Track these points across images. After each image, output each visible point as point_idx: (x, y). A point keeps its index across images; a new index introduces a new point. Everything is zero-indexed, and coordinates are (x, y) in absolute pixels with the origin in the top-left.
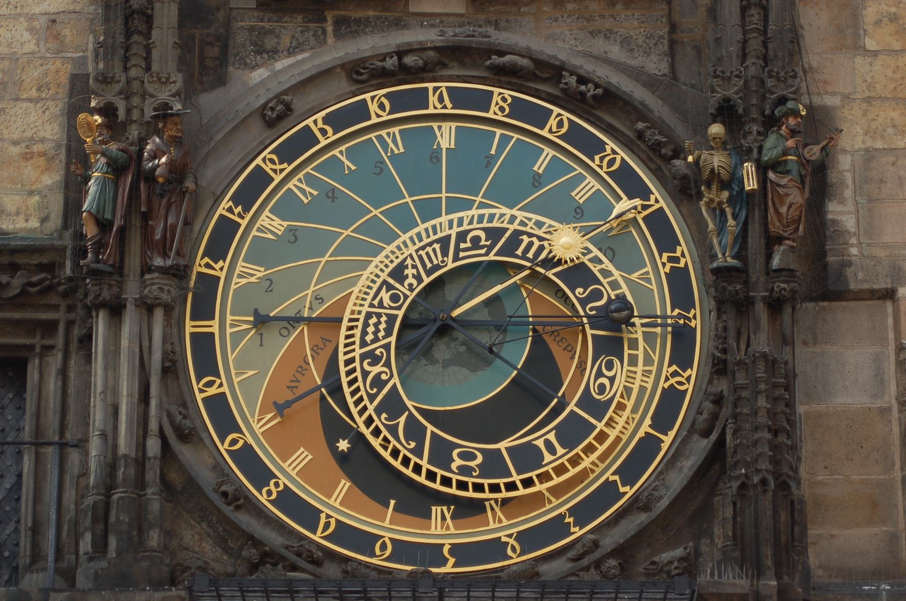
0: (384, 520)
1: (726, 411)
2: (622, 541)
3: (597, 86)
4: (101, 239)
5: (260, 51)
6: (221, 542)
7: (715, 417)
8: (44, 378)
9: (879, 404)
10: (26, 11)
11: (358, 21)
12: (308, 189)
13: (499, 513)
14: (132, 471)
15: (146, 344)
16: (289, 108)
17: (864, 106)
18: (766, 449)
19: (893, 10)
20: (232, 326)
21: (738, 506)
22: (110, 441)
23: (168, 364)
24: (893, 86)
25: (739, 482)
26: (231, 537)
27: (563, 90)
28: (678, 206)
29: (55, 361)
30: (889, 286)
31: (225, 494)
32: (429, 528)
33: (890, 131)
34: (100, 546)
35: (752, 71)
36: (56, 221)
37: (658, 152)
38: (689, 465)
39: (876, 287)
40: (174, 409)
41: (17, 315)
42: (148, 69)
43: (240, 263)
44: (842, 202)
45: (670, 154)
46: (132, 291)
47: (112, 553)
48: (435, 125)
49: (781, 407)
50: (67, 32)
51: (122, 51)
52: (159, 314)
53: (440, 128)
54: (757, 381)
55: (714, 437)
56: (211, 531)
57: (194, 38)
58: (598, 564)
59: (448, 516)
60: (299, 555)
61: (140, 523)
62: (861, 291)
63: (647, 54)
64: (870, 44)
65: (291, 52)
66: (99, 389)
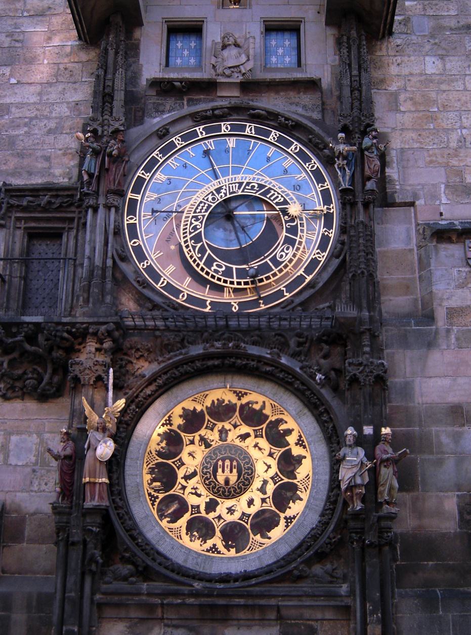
0: (204, 293)
1: (346, 247)
2: (303, 300)
3: (293, 121)
4: (90, 181)
5: (157, 111)
6: (137, 301)
7: (342, 250)
9: (409, 247)
10: (67, 100)
11: (197, 100)
12: (175, 164)
14: (100, 272)
15: (107, 222)
16: (168, 132)
17: (400, 132)
18: (363, 260)
19: (411, 96)
20: (144, 217)
21: (352, 283)
23: (116, 230)
24: (412, 124)
25: (352, 274)
26: (141, 299)
27: (279, 123)
29: (73, 233)
30: (412, 201)
31: (138, 282)
32: (223, 297)
33: (411, 141)
34: (87, 301)
35: (356, 114)
37: (317, 146)
39: (407, 201)
40: (118, 248)
41: (58, 215)
42: (111, 115)
43: (148, 192)
44: (393, 168)
45: (322, 147)
46: (102, 200)
47: (91, 305)
48: (227, 139)
49: (369, 244)
51: (101, 109)
52: (113, 210)
53: (229, 139)
54: (359, 232)
55: (341, 258)
56: (133, 297)
58: (293, 309)
60: (169, 306)
61: (103, 293)
63: (313, 112)
64: (402, 109)
65: (169, 111)
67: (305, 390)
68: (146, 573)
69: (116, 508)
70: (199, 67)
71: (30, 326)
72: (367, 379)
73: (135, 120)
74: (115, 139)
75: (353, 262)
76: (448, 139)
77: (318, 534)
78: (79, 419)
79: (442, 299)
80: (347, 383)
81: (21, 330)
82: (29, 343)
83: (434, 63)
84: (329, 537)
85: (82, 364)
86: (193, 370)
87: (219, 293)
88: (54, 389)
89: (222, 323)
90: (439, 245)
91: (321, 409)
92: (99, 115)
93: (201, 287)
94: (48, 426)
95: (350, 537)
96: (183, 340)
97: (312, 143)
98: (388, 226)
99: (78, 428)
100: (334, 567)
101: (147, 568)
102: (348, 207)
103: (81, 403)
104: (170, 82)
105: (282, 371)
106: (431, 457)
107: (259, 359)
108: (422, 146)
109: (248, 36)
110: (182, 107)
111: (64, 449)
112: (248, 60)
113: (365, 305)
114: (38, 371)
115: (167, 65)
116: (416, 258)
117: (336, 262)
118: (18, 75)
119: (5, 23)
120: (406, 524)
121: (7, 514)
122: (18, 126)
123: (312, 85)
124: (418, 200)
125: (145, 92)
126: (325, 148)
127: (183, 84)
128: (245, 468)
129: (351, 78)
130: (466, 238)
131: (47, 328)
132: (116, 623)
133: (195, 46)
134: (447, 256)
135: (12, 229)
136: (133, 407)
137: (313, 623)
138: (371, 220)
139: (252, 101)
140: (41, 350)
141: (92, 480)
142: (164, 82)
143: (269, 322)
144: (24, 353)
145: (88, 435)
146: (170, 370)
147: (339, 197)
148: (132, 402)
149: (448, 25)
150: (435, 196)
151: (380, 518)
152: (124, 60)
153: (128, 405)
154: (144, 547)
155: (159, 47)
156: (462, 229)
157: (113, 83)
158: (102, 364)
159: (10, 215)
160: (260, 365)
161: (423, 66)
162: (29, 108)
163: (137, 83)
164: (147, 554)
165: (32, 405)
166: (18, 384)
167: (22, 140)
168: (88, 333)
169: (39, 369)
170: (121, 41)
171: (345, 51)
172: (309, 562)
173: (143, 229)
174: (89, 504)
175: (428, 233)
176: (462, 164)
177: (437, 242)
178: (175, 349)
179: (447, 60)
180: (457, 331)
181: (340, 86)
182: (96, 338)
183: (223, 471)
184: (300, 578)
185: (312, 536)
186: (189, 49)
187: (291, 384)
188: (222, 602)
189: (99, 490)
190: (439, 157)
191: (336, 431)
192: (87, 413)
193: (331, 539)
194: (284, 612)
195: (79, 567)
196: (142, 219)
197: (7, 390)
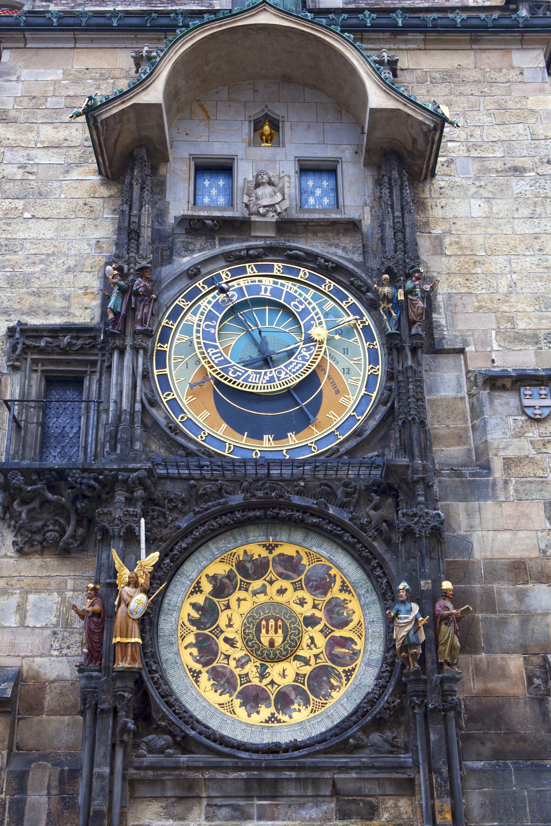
0: (242, 440)
3: (333, 263)
5: (186, 251)
6: (168, 449)
7: (389, 396)
8: (91, 386)
9: (460, 395)
11: (229, 239)
13: (294, 438)
14: (128, 417)
15: (135, 365)
17: (447, 276)
19: (457, 240)
22: (119, 406)
27: (318, 265)
28: (369, 312)
29: (96, 377)
31: (170, 428)
33: (459, 286)
34: (114, 448)
35: (400, 256)
36: (97, 320)
37: (359, 290)
38: (378, 417)
40: (147, 392)
41: (79, 358)
44: (440, 314)
46: (129, 341)
47: (118, 451)
50: (104, 246)
51: (126, 246)
52: (141, 352)
55: (389, 405)
56: (164, 444)
57: (158, 247)
58: (340, 457)
59: (271, 439)
60: (204, 454)
62: (450, 349)
64: (448, 253)
65: (200, 251)
66: (114, 383)
67: (356, 543)
68: (184, 744)
69: (151, 672)
70: (231, 204)
71: (53, 473)
72: (423, 531)
73: (162, 259)
74: (142, 277)
75: (400, 408)
76: (498, 285)
77: (376, 698)
78: (108, 573)
79: (497, 449)
80: (400, 535)
81: (41, 477)
82: (50, 492)
83: (480, 206)
84: (387, 702)
85: (111, 514)
86: (232, 522)
87: (258, 441)
88: (78, 542)
89: (263, 471)
90: (493, 393)
91: (374, 563)
92: (125, 252)
93: (238, 435)
94: (70, 584)
95: (411, 701)
96: (220, 489)
97: (354, 286)
98: (438, 374)
99: (108, 584)
100: (394, 735)
101: (186, 737)
102: (395, 353)
103: (109, 556)
104: (201, 220)
105: (329, 523)
106: (493, 616)
107: (305, 510)
108: (469, 291)
109: (282, 175)
110: (214, 247)
111: (92, 605)
112: (284, 199)
113: (417, 453)
114: (60, 523)
115: (195, 204)
116: (468, 406)
117: (383, 409)
118: (33, 209)
119: (16, 154)
120: (470, 687)
121: (24, 682)
122: (34, 263)
123: (353, 226)
124: (468, 346)
125: (173, 230)
126: (368, 291)
127: (215, 222)
128: (291, 628)
129: (394, 219)
130: (520, 386)
131: (71, 474)
132: (150, 803)
133: (224, 185)
134: (501, 404)
135: (27, 372)
136: (167, 561)
137: (372, 799)
138: (419, 364)
139: (289, 241)
140: (63, 499)
141: (125, 640)
142: (195, 220)
143: (315, 471)
144: (45, 502)
145: (118, 591)
146: (207, 522)
147: (384, 341)
148: (166, 555)
149: (494, 167)
150: (486, 343)
151: (443, 681)
152: (150, 195)
153: (161, 559)
154: (181, 715)
155: (187, 185)
156: (517, 376)
157: (139, 220)
158: (133, 515)
159: (26, 356)
160: (305, 516)
161: (468, 209)
162: (45, 244)
163: (164, 221)
164: (186, 723)
165: (51, 561)
166: (38, 537)
167: (38, 278)
168: (118, 480)
169: (62, 521)
170: (147, 176)
171: (387, 192)
172: (365, 730)
173: (173, 373)
174: (122, 665)
175: (480, 380)
176: (513, 310)
177: (491, 390)
178: (213, 499)
179: (494, 203)
180: (516, 483)
181: (382, 226)
182: (125, 486)
183: (267, 632)
184: (357, 748)
185: (369, 701)
186: (218, 187)
187: (340, 537)
188: (270, 775)
189: (132, 651)
190: (489, 302)
191: (391, 587)
192: (117, 566)
193: (389, 704)
194: (339, 786)
195: (110, 737)
196: (173, 362)
197: (25, 544)
